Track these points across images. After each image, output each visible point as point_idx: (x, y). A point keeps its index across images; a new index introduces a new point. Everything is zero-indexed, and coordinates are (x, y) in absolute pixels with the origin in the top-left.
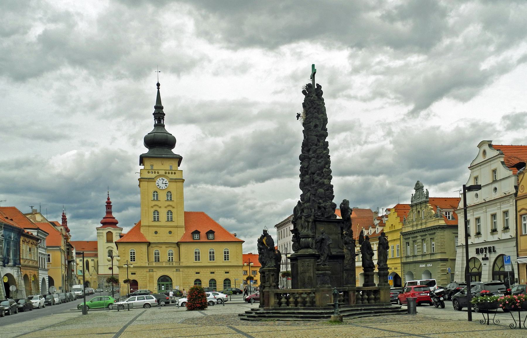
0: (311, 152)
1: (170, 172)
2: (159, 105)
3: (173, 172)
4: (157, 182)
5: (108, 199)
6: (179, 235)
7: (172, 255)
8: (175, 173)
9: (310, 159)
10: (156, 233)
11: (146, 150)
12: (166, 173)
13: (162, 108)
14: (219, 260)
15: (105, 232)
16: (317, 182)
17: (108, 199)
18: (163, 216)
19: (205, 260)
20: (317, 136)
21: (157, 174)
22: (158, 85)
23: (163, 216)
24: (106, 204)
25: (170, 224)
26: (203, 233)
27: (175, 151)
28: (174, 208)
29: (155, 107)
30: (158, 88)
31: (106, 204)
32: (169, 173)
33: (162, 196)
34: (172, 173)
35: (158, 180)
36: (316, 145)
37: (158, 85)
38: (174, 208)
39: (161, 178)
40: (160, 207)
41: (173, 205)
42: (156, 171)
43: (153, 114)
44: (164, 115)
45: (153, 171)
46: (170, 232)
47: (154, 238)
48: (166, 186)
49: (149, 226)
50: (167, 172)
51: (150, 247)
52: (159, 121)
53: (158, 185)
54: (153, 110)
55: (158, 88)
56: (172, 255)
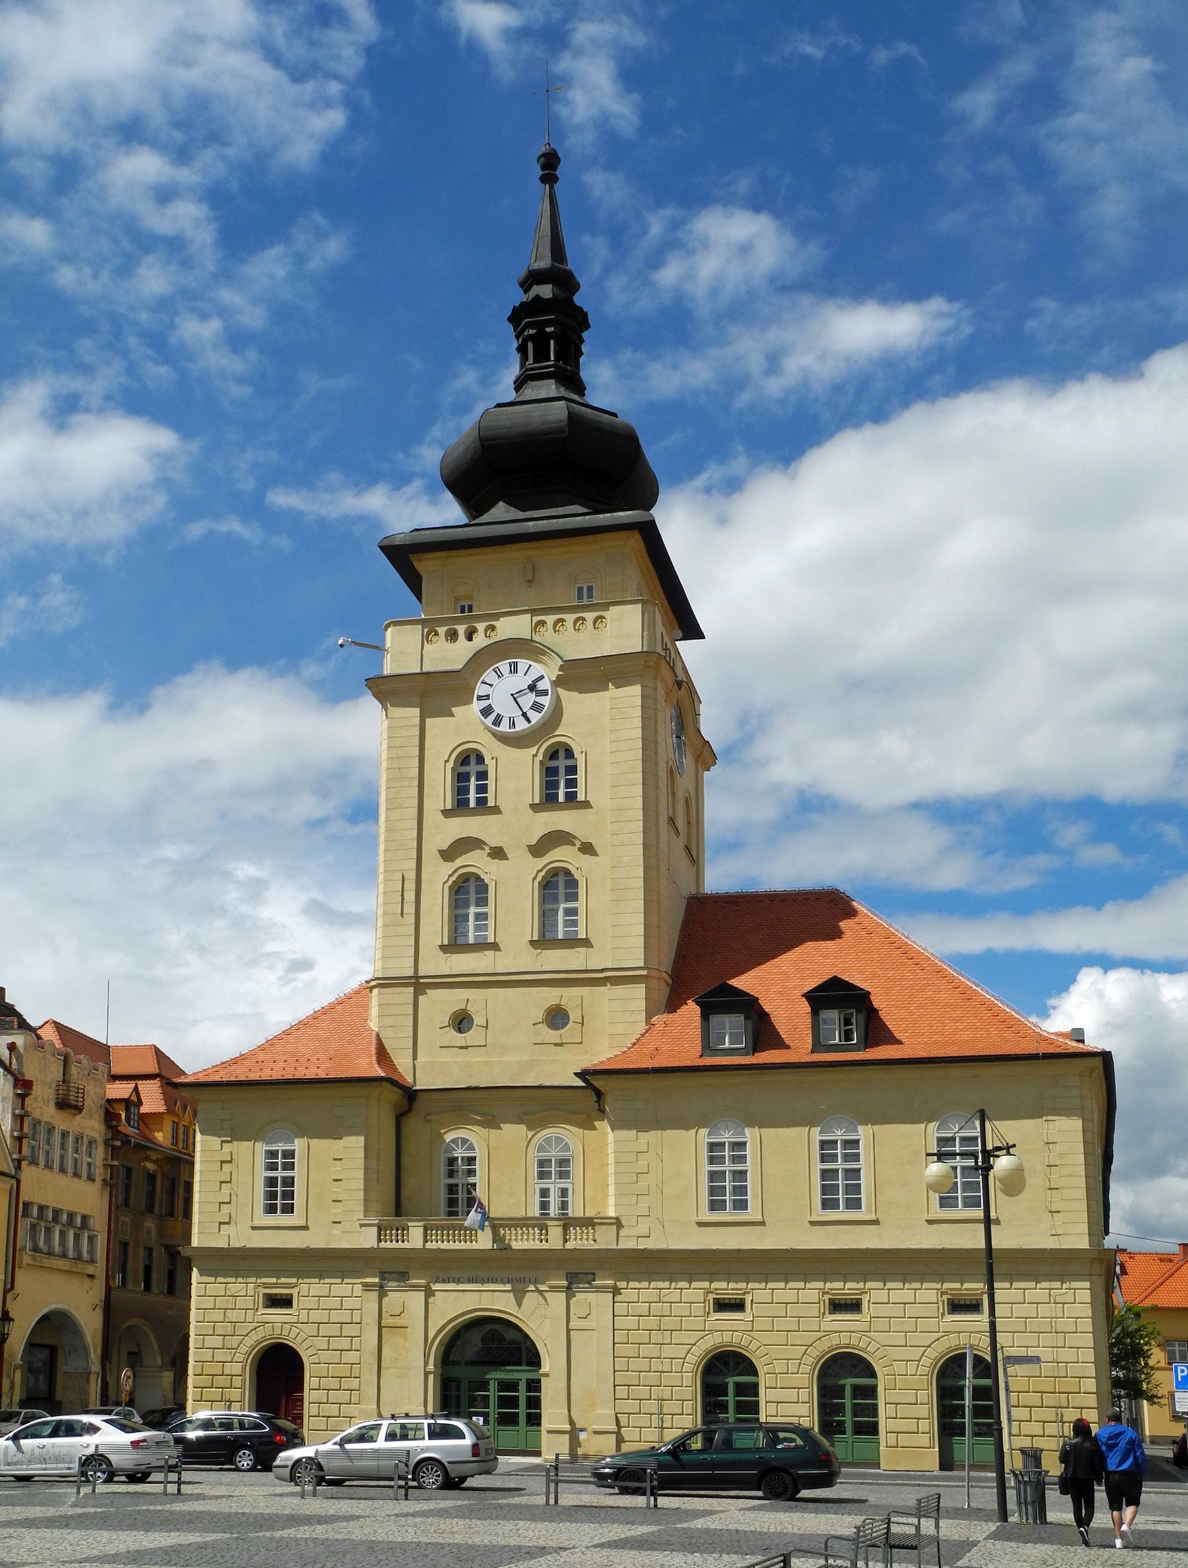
4: (481, 690)
6: (618, 1025)
7: (563, 1175)
10: (462, 1021)
21: (480, 641)
33: (515, 775)
35: (489, 675)
39: (504, 666)
40: (498, 853)
41: (584, 835)
47: (447, 1057)
48: (537, 707)
49: (419, 984)
51: (413, 1125)
53: (486, 712)
56: (563, 1175)
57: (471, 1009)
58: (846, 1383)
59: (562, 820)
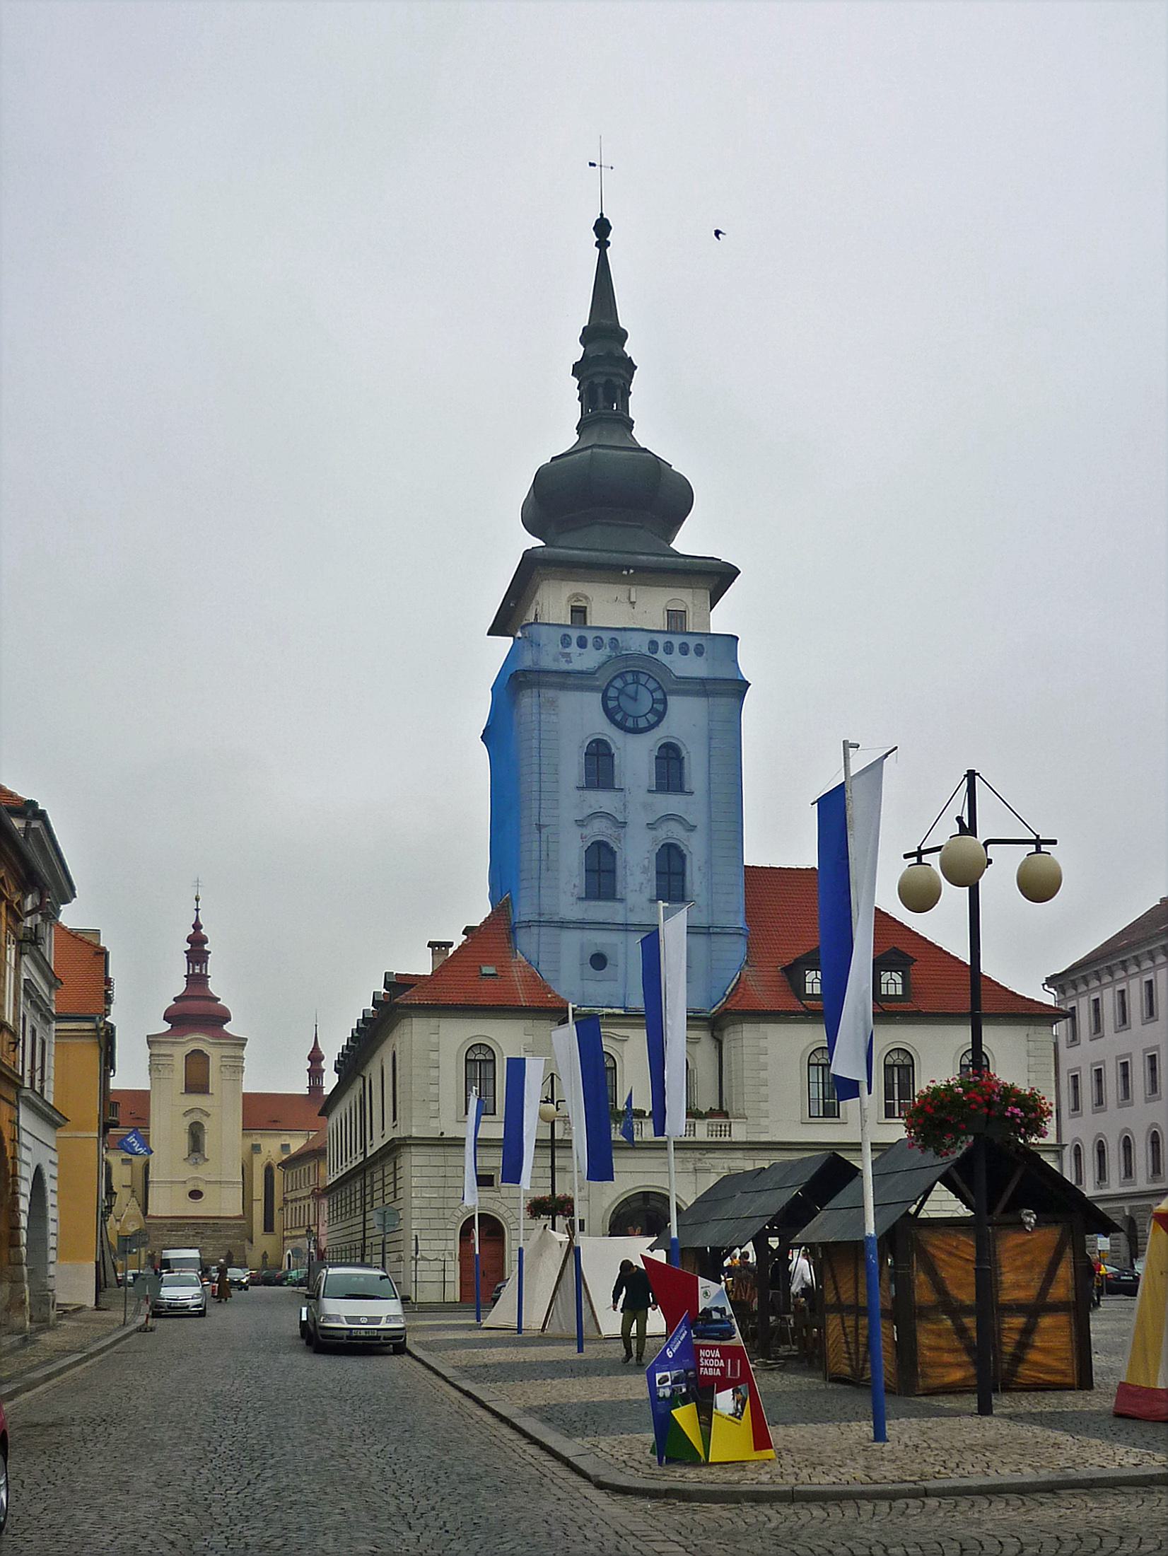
1: (677, 640)
3: (692, 642)
5: (197, 926)
8: (699, 651)
10: (599, 961)
12: (653, 645)
17: (197, 926)
24: (188, 946)
28: (692, 828)
30: (603, 244)
31: (188, 946)
32: (669, 649)
34: (684, 649)
38: (692, 828)
42: (606, 636)
44: (630, 367)
45: (590, 636)
50: (661, 640)
55: (603, 244)
57: (608, 953)
59: (671, 803)
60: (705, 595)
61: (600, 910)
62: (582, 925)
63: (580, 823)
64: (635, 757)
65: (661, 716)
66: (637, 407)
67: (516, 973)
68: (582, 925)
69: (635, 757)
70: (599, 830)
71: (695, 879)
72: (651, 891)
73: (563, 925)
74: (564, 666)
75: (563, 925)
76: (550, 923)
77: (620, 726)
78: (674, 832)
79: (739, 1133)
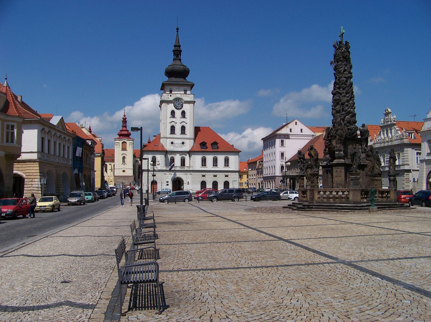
0: (341, 89)
2: (177, 44)
5: (125, 116)
9: (341, 94)
10: (172, 143)
11: (166, 79)
13: (179, 46)
14: (221, 166)
15: (121, 142)
16: (346, 111)
18: (178, 130)
19: (210, 166)
20: (345, 77)
22: (178, 29)
23: (178, 130)
25: (183, 136)
26: (209, 145)
27: (189, 79)
28: (187, 123)
29: (175, 46)
30: (177, 32)
36: (345, 84)
37: (178, 29)
38: (187, 123)
43: (173, 51)
46: (183, 143)
52: (177, 56)
54: (173, 48)
58: (215, 184)
59: (183, 120)
60: (190, 88)
61: (173, 136)
62: (169, 138)
63: (170, 123)
64: (178, 113)
65: (182, 107)
66: (182, 57)
67: (160, 145)
68: (169, 138)
69: (178, 113)
70: (173, 124)
71: (187, 131)
72: (180, 132)
73: (167, 138)
74: (168, 99)
75: (167, 138)
76: (165, 138)
77: (176, 108)
78: (183, 124)
79: (191, 169)
